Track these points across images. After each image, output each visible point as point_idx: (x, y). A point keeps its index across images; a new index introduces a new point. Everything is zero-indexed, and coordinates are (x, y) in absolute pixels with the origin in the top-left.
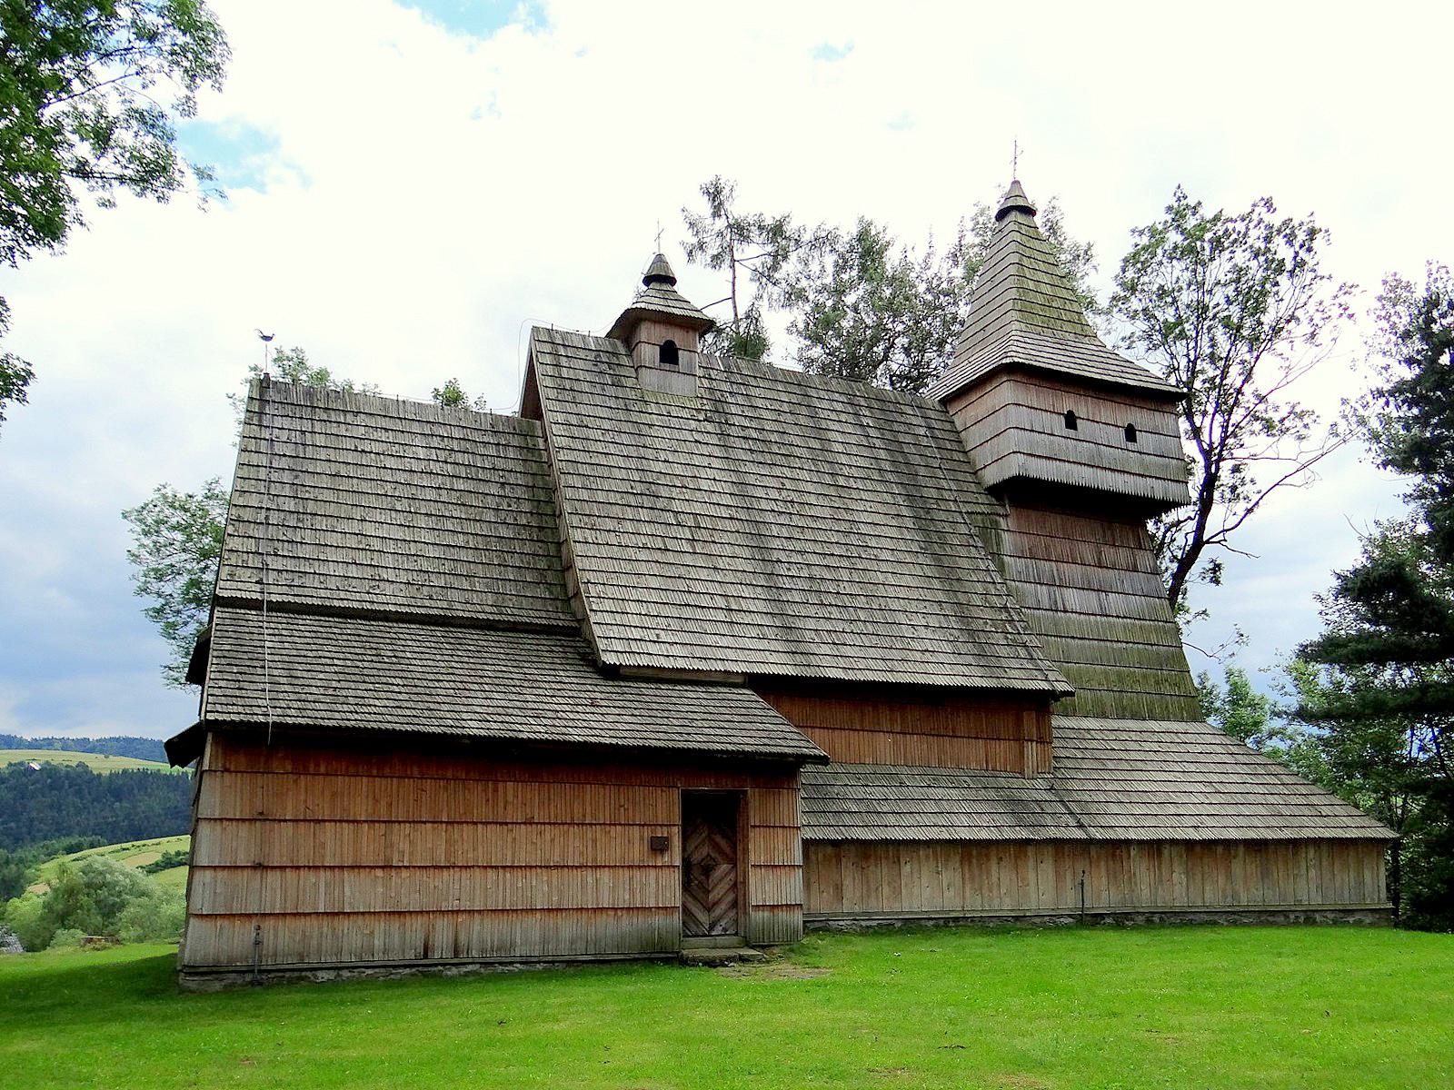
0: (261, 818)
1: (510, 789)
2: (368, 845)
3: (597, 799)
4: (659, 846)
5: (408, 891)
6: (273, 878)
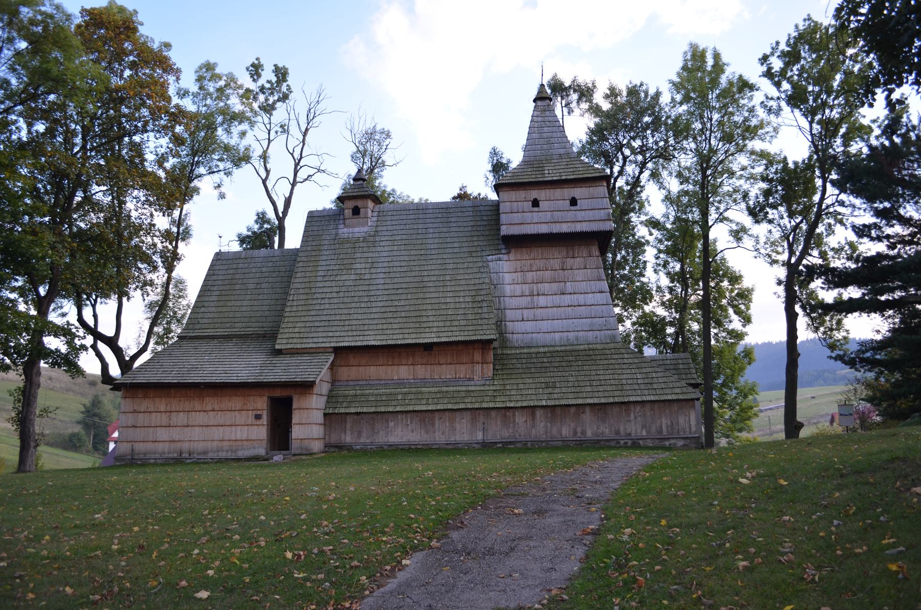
0: (134, 412)
1: (207, 399)
2: (163, 419)
3: (236, 402)
4: (258, 417)
5: (175, 434)
6: (138, 429)
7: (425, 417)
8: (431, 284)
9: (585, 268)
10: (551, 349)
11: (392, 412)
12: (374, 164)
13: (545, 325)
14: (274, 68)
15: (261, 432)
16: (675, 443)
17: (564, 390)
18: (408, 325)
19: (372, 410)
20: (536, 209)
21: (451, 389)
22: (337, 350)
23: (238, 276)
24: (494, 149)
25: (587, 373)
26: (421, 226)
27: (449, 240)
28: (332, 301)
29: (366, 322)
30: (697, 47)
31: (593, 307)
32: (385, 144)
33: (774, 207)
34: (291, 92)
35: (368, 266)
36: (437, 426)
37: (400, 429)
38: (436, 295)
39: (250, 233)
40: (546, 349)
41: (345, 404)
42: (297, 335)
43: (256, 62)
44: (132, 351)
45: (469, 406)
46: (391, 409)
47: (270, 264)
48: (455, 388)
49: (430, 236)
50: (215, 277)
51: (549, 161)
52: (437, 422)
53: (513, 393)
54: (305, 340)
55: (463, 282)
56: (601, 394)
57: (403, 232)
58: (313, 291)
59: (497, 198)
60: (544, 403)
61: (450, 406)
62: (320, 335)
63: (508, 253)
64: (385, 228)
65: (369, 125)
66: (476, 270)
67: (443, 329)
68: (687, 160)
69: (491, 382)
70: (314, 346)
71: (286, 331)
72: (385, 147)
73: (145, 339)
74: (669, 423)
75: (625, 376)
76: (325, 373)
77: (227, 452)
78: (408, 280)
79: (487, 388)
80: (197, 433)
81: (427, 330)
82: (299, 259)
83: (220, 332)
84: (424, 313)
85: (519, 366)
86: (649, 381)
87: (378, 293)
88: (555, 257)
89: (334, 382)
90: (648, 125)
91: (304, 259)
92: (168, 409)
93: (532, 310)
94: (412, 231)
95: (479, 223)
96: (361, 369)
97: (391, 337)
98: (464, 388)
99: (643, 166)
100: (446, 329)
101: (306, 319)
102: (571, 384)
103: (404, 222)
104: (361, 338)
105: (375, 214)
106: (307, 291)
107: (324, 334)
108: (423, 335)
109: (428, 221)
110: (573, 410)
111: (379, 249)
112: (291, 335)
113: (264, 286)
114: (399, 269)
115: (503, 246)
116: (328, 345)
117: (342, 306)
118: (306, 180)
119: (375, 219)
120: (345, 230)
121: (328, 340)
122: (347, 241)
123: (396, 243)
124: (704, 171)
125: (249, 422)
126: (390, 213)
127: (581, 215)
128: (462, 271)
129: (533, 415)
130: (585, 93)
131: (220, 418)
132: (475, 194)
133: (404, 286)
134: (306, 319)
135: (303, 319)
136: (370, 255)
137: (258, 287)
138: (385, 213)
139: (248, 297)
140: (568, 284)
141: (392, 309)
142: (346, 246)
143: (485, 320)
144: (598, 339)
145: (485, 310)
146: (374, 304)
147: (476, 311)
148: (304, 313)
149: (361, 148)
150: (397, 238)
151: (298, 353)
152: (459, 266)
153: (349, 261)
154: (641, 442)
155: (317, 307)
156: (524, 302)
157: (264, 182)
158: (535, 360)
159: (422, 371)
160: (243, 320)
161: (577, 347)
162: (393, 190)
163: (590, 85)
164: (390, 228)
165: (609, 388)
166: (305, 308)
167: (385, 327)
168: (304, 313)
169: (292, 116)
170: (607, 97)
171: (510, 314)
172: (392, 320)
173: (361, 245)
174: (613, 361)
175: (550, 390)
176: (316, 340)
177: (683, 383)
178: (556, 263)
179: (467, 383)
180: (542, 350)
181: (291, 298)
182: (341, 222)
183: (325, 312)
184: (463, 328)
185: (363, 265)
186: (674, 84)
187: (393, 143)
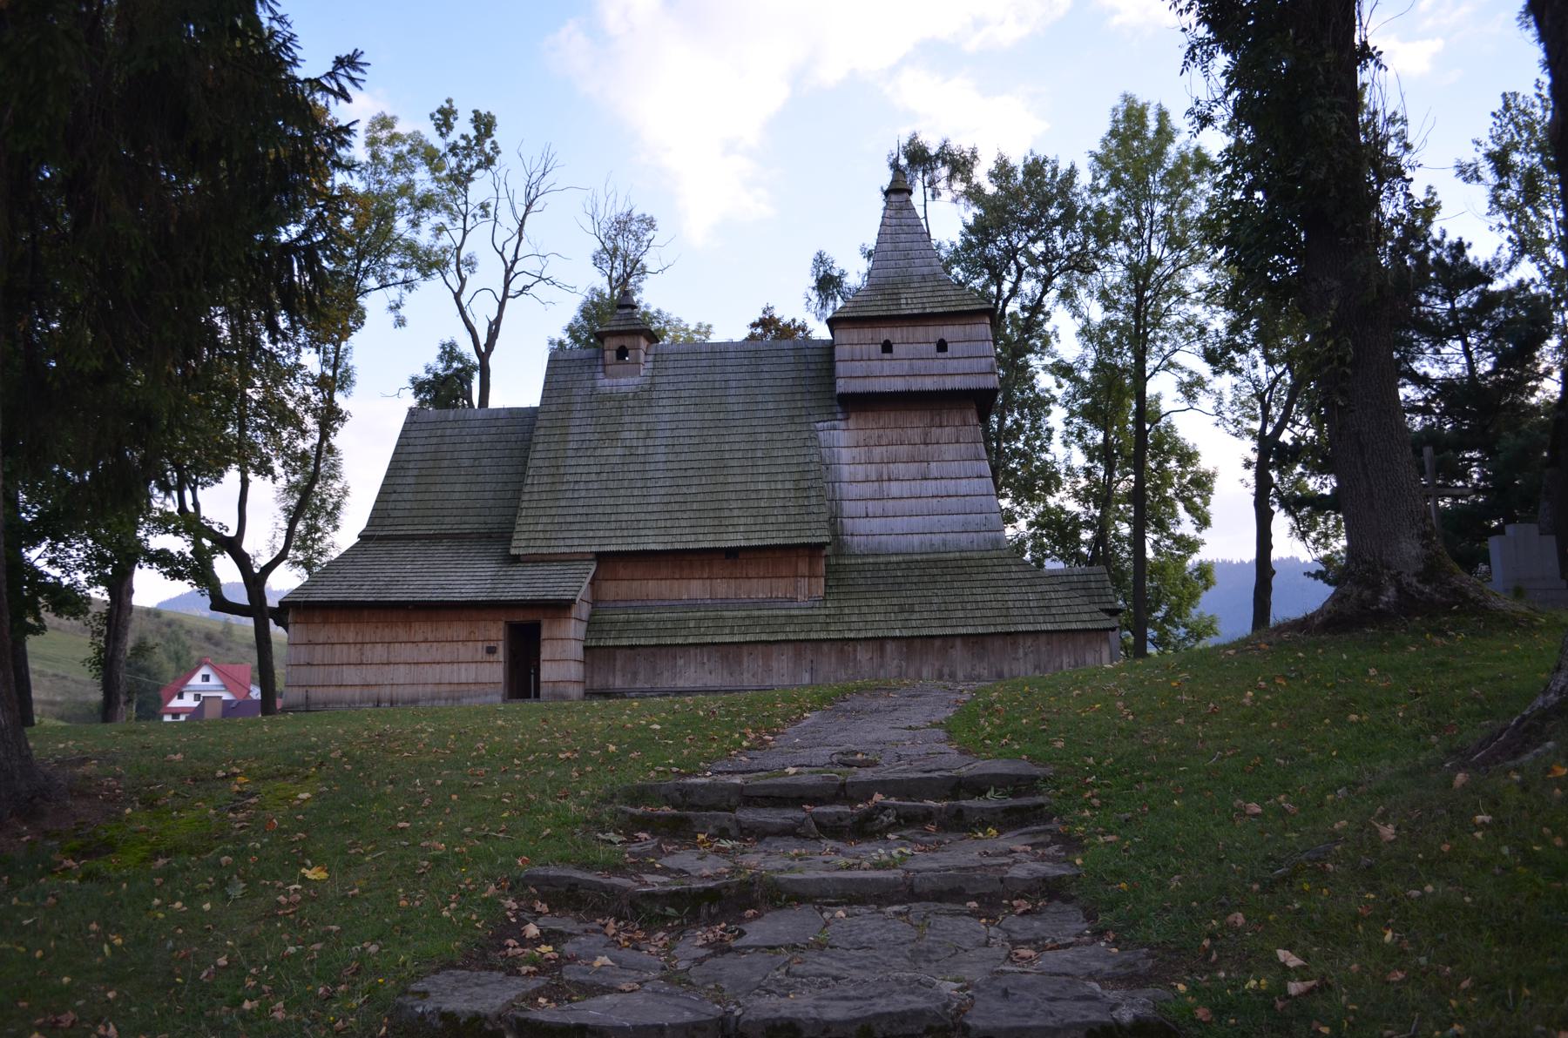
0: (309, 643)
1: (416, 626)
2: (353, 654)
3: (459, 630)
4: (491, 651)
5: (370, 674)
7: (729, 652)
8: (735, 463)
9: (957, 442)
10: (907, 558)
11: (682, 645)
12: (628, 270)
13: (899, 524)
14: (472, 115)
15: (495, 672)
17: (925, 615)
18: (702, 522)
19: (654, 641)
20: (887, 356)
21: (765, 612)
22: (601, 558)
23: (445, 448)
24: (820, 255)
25: (958, 592)
26: (718, 377)
27: (760, 398)
28: (590, 486)
29: (642, 516)
30: (1134, 101)
32: (646, 238)
33: (1242, 350)
34: (498, 153)
35: (642, 435)
36: (745, 665)
37: (693, 669)
38: (743, 479)
39: (430, 376)
40: (900, 558)
41: (613, 634)
42: (541, 535)
43: (446, 106)
44: (263, 560)
45: (792, 637)
46: (680, 641)
47: (493, 430)
48: (770, 612)
49: (733, 392)
50: (410, 449)
51: (907, 284)
52: (745, 659)
53: (854, 618)
54: (553, 543)
55: (781, 461)
56: (977, 622)
57: (691, 386)
58: (562, 471)
59: (829, 337)
60: (897, 633)
61: (764, 637)
62: (575, 534)
63: (847, 419)
64: (665, 380)
65: (621, 209)
66: (799, 443)
67: (753, 528)
68: (1114, 275)
69: (823, 604)
70: (567, 550)
71: (525, 528)
72: (646, 243)
73: (283, 541)
74: (1073, 663)
75: (1012, 597)
76: (584, 590)
77: (446, 699)
78: (701, 456)
79: (816, 612)
80: (401, 674)
81: (731, 529)
82: (538, 424)
83: (423, 529)
84: (725, 505)
85: (861, 581)
86: (1046, 603)
87: (658, 475)
88: (914, 426)
89: (595, 602)
90: (1056, 222)
91: (545, 423)
92: (359, 639)
93: (881, 502)
94: (705, 385)
95: (803, 374)
96: (635, 584)
97: (678, 538)
98: (784, 612)
99: (1047, 282)
100: (758, 528)
101: (553, 512)
102: (935, 607)
103: (694, 371)
104: (635, 540)
105: (650, 358)
106: (553, 470)
107: (581, 534)
108: (725, 536)
109: (730, 369)
110: (938, 643)
111: (657, 410)
112: (532, 535)
113: (484, 462)
114: (687, 441)
115: (839, 409)
116: (587, 549)
117: (606, 493)
118: (521, 292)
119: (650, 365)
120: (606, 381)
121: (587, 542)
122: (610, 397)
123: (682, 402)
124: (1139, 292)
125: (479, 658)
126: (672, 357)
127: (952, 366)
128: (779, 445)
129: (882, 650)
130: (961, 166)
131: (436, 652)
132: (787, 319)
133: (695, 465)
134: (553, 512)
135: (549, 512)
136: (644, 418)
137: (477, 463)
138: (665, 357)
139: (462, 479)
140: (933, 465)
141: (678, 499)
142: (608, 405)
143: (814, 516)
145: (814, 501)
146: (652, 491)
147: (801, 502)
148: (551, 504)
149: (609, 245)
150: (683, 394)
151: (543, 561)
152: (775, 437)
153: (614, 428)
155: (569, 495)
156: (868, 489)
157: (457, 296)
158: (885, 574)
159: (723, 588)
160: (455, 512)
161: (945, 555)
162: (659, 312)
163: (968, 155)
164: (672, 379)
165: (989, 613)
166: (551, 496)
167: (669, 524)
168: (551, 504)
169: (502, 193)
170: (991, 174)
171: (848, 507)
172: (679, 515)
173: (631, 403)
174: (995, 576)
175: (906, 615)
176: (569, 542)
177: (1096, 608)
178: (915, 434)
179: (787, 605)
180: (894, 559)
181: (529, 481)
182: (600, 369)
183: (581, 502)
184: (782, 527)
185: (634, 434)
186: (1097, 158)
187: (659, 236)
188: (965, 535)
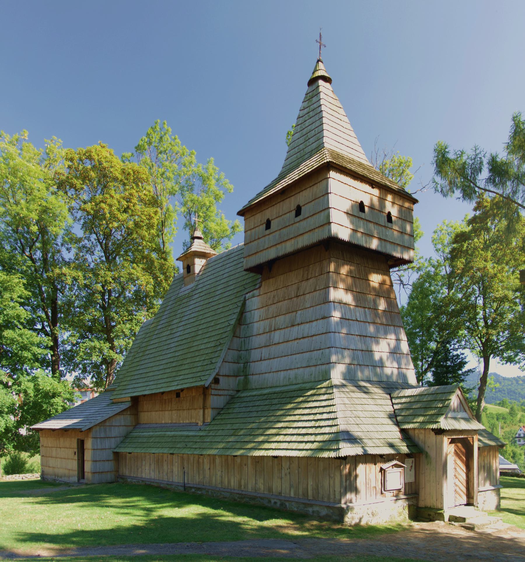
16: (318, 511)
31: (314, 338)
140: (299, 312)
144: (313, 376)
154: (287, 504)
188: (308, 369)
